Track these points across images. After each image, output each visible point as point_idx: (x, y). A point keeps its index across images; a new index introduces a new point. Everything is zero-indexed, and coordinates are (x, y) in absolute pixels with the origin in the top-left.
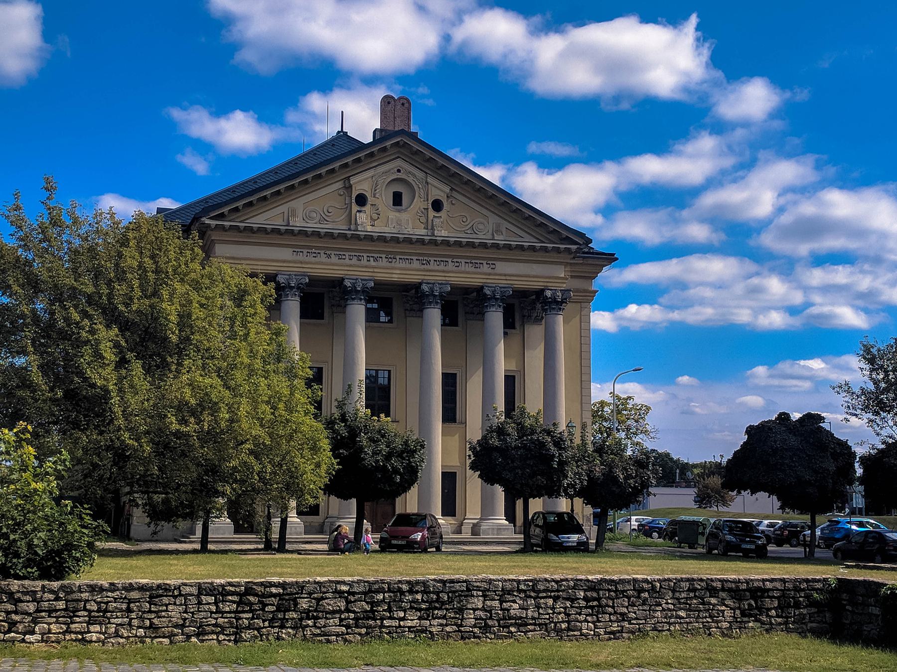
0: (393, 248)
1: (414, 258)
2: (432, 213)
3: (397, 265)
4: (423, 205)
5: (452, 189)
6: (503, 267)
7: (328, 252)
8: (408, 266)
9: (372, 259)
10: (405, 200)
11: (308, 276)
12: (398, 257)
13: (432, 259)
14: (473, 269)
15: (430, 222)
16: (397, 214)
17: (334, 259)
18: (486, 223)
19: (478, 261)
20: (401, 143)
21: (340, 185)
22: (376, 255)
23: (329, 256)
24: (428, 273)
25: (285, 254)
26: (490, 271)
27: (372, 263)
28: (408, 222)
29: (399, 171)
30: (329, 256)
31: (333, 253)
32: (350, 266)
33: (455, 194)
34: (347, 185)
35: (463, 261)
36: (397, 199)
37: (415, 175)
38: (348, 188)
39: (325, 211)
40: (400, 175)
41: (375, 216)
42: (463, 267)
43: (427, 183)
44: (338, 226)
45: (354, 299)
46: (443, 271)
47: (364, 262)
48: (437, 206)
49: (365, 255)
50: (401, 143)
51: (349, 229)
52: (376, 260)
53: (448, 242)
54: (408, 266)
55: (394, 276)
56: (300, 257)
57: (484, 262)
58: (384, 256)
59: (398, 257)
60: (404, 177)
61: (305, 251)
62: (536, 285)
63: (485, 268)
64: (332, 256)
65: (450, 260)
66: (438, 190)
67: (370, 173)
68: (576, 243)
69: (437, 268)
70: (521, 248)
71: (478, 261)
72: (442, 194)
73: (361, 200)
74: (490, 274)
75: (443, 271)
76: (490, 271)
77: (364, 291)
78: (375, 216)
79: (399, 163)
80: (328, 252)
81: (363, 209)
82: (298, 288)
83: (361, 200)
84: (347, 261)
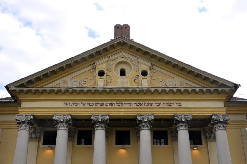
0: (120, 97)
1: (133, 102)
2: (141, 77)
3: (123, 106)
4: (136, 74)
5: (152, 64)
6: (185, 104)
7: (83, 102)
8: (129, 106)
9: (108, 105)
12: (123, 102)
13: (143, 103)
14: (168, 106)
15: (140, 81)
16: (122, 79)
17: (87, 106)
18: (173, 81)
19: (171, 102)
20: (122, 42)
22: (111, 102)
23: (84, 104)
24: (141, 110)
25: (60, 104)
26: (178, 106)
27: (109, 106)
29: (123, 58)
30: (84, 104)
31: (86, 102)
32: (96, 108)
33: (155, 67)
34: (94, 67)
35: (162, 102)
36: (123, 73)
39: (82, 81)
40: (123, 60)
41: (109, 81)
42: (162, 106)
43: (138, 62)
45: (98, 127)
46: (150, 108)
47: (104, 106)
48: (144, 73)
49: (105, 103)
50: (122, 42)
52: (111, 104)
53: (150, 91)
54: (129, 106)
55: (121, 113)
56: (68, 106)
57: (175, 102)
58: (115, 102)
59: (123, 102)
60: (125, 60)
61: (71, 103)
62: (207, 113)
63: (175, 106)
64: (86, 104)
65: (154, 102)
66: (145, 65)
67: (106, 59)
69: (146, 107)
70: (194, 91)
71: (171, 102)
72: (147, 67)
75: (150, 108)
76: (178, 106)
77: (103, 122)
79: (123, 54)
80: (83, 102)
81: (102, 77)
82: (66, 123)
83: (101, 74)
84: (94, 106)
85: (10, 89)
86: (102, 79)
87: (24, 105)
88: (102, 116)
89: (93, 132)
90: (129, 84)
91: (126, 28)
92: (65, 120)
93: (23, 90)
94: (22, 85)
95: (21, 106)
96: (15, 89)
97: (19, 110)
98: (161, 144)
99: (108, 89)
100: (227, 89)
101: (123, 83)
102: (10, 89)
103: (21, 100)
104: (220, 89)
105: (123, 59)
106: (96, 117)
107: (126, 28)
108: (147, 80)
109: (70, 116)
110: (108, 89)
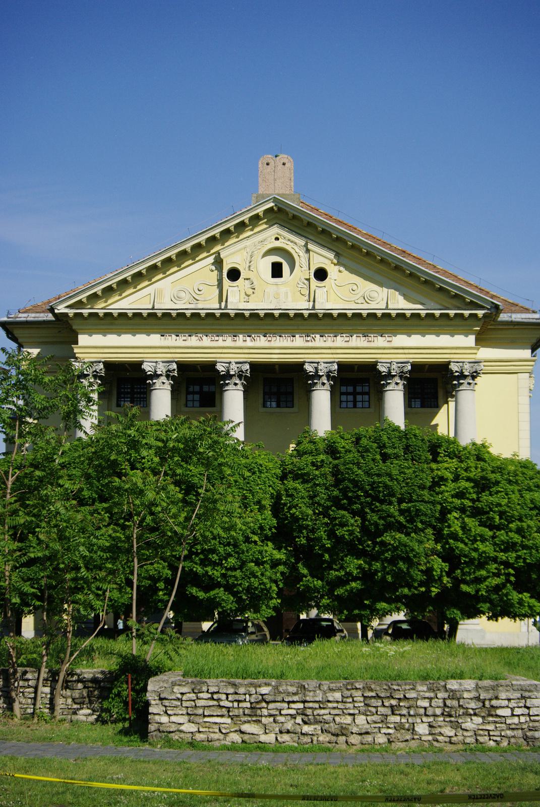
2: (314, 282)
6: (401, 340)
10: (286, 268)
11: (176, 362)
21: (211, 260)
25: (155, 339)
28: (287, 295)
29: (277, 239)
36: (277, 271)
37: (293, 243)
38: (218, 263)
40: (277, 244)
41: (250, 292)
43: (308, 251)
44: (209, 303)
48: (321, 274)
51: (220, 309)
66: (322, 257)
68: (482, 308)
72: (327, 261)
73: (234, 274)
74: (384, 348)
78: (250, 292)
83: (234, 274)
85: (56, 311)
86: (236, 288)
87: (83, 339)
88: (237, 363)
89: (217, 396)
90: (290, 299)
91: (284, 164)
92: (164, 372)
93: (81, 314)
94: (79, 304)
95: (77, 343)
96: (66, 311)
97: (76, 351)
98: (355, 406)
99: (249, 312)
100: (480, 313)
101: (277, 296)
102: (56, 311)
103: (78, 331)
104: (466, 313)
105: (277, 242)
106: (224, 365)
107: (284, 164)
108: (325, 289)
109: (174, 364)
110: (249, 312)
